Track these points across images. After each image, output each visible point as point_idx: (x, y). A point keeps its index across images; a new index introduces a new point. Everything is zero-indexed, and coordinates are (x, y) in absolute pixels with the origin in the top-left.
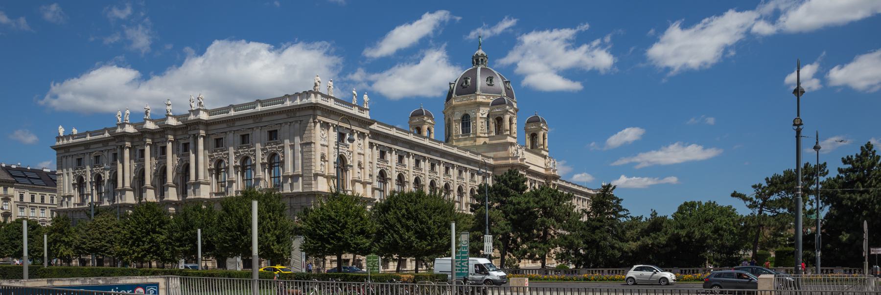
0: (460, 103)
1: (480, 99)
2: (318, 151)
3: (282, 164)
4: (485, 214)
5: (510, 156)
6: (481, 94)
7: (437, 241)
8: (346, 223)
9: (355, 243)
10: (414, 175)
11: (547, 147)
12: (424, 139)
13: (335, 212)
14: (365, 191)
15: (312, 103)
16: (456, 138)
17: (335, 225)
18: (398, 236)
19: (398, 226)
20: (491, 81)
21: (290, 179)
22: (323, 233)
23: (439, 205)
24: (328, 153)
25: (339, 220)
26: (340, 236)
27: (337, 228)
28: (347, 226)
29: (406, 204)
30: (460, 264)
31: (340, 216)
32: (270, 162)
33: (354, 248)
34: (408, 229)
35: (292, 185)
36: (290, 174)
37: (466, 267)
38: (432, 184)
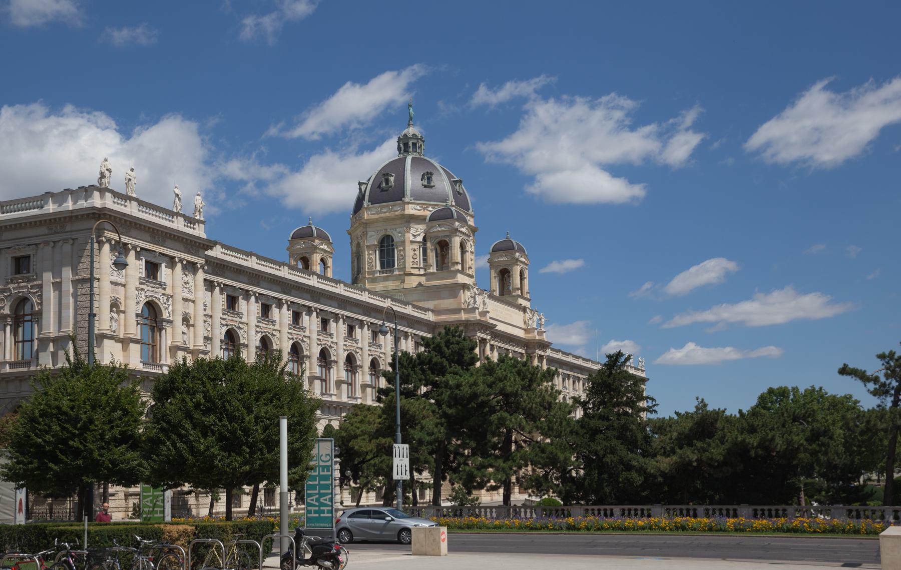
0: (376, 216)
1: (410, 210)
2: (105, 293)
3: (37, 317)
4: (395, 407)
5: (463, 306)
6: (413, 201)
7: (262, 454)
8: (91, 421)
9: (111, 461)
10: (224, 325)
11: (527, 293)
12: (280, 267)
13: (71, 400)
14: (127, 356)
15: (94, 208)
16: (371, 276)
17: (68, 426)
18: (185, 447)
19: (187, 426)
20: (429, 179)
21: (51, 344)
22: (44, 441)
23: (269, 386)
24: (125, 298)
25: (77, 415)
26: (77, 448)
27: (68, 431)
28: (92, 427)
29: (203, 383)
30: (318, 500)
31: (79, 408)
32: (15, 313)
33: (107, 468)
34: (205, 431)
35: (54, 355)
36: (52, 336)
37: (328, 505)
38: (265, 342)
